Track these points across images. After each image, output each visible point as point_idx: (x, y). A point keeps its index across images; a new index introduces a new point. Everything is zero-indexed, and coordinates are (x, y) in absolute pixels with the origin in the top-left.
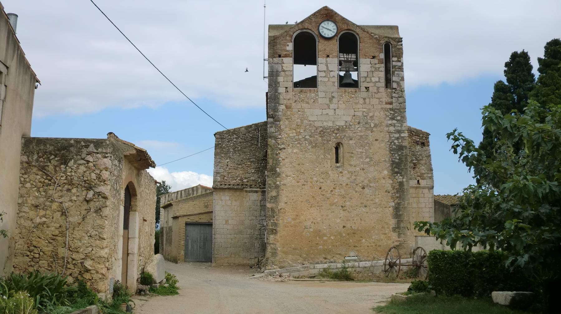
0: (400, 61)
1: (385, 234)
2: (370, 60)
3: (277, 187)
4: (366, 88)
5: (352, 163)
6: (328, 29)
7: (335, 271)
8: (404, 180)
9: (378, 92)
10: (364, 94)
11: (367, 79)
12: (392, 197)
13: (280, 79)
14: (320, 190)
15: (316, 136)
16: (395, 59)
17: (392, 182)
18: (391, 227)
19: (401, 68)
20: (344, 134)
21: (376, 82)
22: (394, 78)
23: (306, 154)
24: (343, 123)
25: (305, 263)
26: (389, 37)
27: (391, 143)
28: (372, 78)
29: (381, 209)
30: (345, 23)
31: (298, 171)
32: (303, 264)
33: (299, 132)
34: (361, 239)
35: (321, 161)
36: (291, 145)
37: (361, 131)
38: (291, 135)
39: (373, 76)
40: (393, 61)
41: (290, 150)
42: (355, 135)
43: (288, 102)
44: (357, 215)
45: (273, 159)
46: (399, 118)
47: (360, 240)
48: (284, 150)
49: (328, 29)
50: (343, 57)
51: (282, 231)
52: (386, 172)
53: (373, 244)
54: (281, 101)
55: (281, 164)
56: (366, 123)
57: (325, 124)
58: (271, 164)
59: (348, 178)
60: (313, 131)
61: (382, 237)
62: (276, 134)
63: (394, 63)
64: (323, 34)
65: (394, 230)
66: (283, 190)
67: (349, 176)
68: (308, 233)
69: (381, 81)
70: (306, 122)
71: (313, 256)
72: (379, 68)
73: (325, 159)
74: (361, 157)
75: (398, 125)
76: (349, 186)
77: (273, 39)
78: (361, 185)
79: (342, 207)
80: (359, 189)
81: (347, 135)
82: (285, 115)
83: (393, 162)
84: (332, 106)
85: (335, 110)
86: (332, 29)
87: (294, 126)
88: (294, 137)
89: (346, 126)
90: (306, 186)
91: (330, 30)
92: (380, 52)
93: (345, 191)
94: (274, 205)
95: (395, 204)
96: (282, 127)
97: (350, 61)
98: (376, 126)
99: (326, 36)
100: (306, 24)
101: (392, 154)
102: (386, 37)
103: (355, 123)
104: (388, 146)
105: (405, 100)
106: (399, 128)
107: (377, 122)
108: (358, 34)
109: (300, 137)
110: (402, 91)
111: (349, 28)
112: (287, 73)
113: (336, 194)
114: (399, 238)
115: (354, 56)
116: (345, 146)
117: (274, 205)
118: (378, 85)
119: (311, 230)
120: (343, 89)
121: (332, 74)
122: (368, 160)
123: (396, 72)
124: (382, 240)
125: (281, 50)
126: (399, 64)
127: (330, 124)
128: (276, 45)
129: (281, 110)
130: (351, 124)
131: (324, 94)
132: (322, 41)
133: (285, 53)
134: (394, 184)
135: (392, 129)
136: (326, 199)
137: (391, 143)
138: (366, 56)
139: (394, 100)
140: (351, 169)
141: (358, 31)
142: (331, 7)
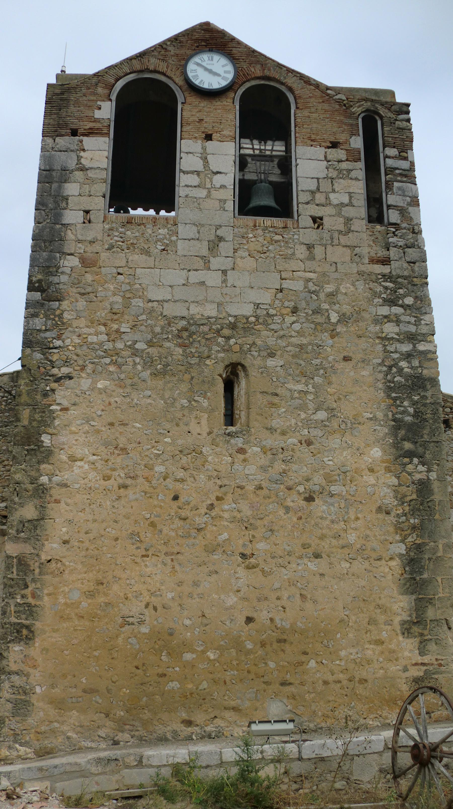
0: (406, 159)
1: (380, 642)
2: (323, 150)
3: (41, 492)
4: (314, 219)
5: (275, 423)
7: (213, 774)
8: (433, 476)
9: (349, 231)
10: (311, 235)
11: (318, 196)
12: (398, 528)
13: (71, 189)
14: (175, 504)
15: (167, 344)
17: (395, 481)
18: (397, 620)
19: (409, 175)
20: (250, 340)
21: (342, 205)
22: (391, 199)
23: (134, 395)
24: (247, 310)
25: (120, 736)
26: (372, 101)
27: (390, 367)
28: (332, 196)
29: (366, 564)
30: (258, 62)
31: (106, 444)
32: (116, 743)
33: (117, 331)
34: (303, 658)
35: (179, 415)
36: (90, 368)
37: (300, 333)
38: (92, 339)
39: (334, 191)
40: (386, 157)
41: (85, 383)
42: (282, 343)
43: (90, 249)
44: (292, 583)
45: (34, 406)
46: (409, 301)
47: (301, 664)
48: (67, 382)
50: (251, 147)
51: (50, 633)
52: (376, 453)
53: (341, 676)
54: (70, 247)
55: (57, 422)
56: (316, 312)
57: (194, 310)
58: (26, 422)
59: (264, 469)
60: (158, 329)
61: (371, 651)
62: (48, 334)
63: (390, 162)
64: (197, 82)
65: (407, 629)
66: (57, 501)
67: (264, 461)
68: (133, 641)
69: (355, 202)
70: (138, 302)
71: (146, 715)
73: (191, 409)
74: (303, 407)
75: (407, 318)
76: (265, 492)
77: (58, 91)
78: (301, 489)
79: (243, 556)
80: (295, 501)
81: (259, 342)
82: (76, 283)
83: (398, 424)
84: (215, 262)
85: (224, 272)
86: (222, 74)
87: (102, 314)
88: (101, 344)
89: (257, 317)
90: (130, 492)
91: (219, 75)
92: (352, 134)
93: (252, 507)
94: (27, 549)
95: (409, 550)
96: (66, 316)
97: (271, 158)
98: (344, 319)
99: (206, 86)
100: (153, 60)
101: (395, 399)
102: (366, 100)
103: (284, 311)
104: (381, 376)
105: (424, 253)
106: (413, 329)
107: (346, 309)
108: (291, 89)
109: (120, 345)
110: (416, 231)
111: (267, 73)
112: (90, 174)
113: (226, 515)
114: (422, 653)
115: (279, 147)
116: (253, 372)
117: (27, 549)
118: (348, 212)
119: (144, 629)
120: (249, 220)
121: (218, 180)
122: (322, 415)
123: (396, 184)
124: (369, 662)
125: (80, 119)
126: (404, 165)
127: (211, 311)
128: (67, 107)
129: (68, 270)
130: (272, 312)
131: (195, 229)
132: (193, 100)
134: (403, 489)
135: (390, 329)
136: (193, 532)
137: (390, 367)
138: (312, 141)
139: (393, 253)
140: (272, 441)
141: (290, 81)
142: (221, 23)
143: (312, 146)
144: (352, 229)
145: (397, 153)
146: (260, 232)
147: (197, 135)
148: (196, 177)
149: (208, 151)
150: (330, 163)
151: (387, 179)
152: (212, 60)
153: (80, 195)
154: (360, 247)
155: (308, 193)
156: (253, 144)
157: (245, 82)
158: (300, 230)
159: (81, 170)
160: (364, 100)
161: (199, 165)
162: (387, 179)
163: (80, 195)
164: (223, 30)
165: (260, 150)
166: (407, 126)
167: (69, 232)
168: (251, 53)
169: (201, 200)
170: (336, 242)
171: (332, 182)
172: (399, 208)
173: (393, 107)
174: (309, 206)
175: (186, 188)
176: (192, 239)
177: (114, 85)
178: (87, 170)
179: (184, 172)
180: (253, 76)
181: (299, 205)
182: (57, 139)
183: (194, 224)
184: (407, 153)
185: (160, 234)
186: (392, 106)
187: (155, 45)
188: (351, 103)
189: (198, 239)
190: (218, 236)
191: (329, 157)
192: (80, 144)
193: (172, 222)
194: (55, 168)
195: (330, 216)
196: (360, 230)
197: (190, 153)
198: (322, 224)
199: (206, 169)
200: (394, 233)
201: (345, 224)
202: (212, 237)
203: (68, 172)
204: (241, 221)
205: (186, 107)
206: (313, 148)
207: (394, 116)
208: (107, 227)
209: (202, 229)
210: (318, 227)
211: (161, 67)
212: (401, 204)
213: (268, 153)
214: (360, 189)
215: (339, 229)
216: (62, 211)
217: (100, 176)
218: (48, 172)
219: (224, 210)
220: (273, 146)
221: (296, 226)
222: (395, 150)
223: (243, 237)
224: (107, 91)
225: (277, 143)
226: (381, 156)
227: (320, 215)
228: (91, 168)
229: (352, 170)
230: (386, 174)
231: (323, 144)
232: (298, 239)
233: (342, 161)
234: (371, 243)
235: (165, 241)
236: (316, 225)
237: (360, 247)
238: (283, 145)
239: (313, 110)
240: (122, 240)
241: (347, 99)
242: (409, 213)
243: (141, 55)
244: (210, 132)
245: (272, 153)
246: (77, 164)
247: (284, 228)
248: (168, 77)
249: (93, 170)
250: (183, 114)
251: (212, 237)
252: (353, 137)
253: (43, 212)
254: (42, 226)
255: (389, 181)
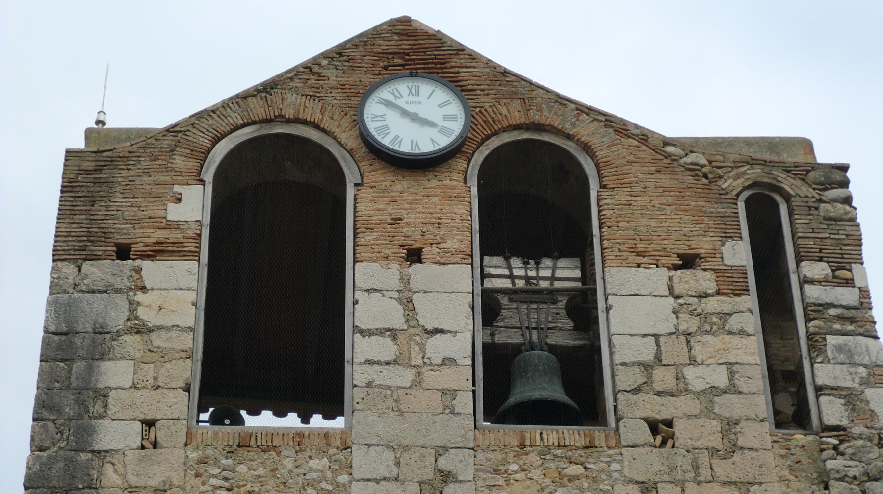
0: (849, 283)
2: (664, 273)
4: (654, 426)
6: (414, 118)
9: (734, 448)
10: (648, 462)
13: (115, 374)
16: (817, 270)
21: (715, 391)
22: (824, 373)
26: (765, 163)
28: (690, 373)
30: (514, 95)
39: (693, 361)
40: (805, 281)
49: (416, 117)
50: (505, 272)
63: (814, 293)
64: (386, 141)
69: (742, 384)
72: (725, 316)
77: (88, 165)
86: (440, 122)
97: (551, 295)
99: (405, 148)
100: (291, 98)
102: (752, 162)
108: (587, 148)
111: (535, 116)
112: (158, 340)
115: (568, 271)
120: (510, 433)
121: (437, 347)
123: (831, 340)
125: (135, 222)
126: (847, 296)
128: (107, 197)
131: (389, 456)
132: (380, 177)
133: (159, 235)
138: (640, 256)
141: (586, 131)
143: (639, 265)
144: (740, 443)
145: (828, 271)
146: (534, 458)
147: (388, 252)
148: (388, 341)
149: (414, 285)
150: (681, 301)
151: (811, 330)
152: (417, 94)
153: (134, 386)
154: (760, 483)
155: (636, 368)
156: (510, 268)
157: (488, 137)
158: (624, 450)
159: (137, 333)
160: (748, 163)
161: (396, 318)
162: (811, 330)
163: (134, 386)
164: (438, 31)
165: (527, 279)
166: (847, 213)
167: (109, 469)
168: (500, 77)
169: (401, 392)
170: (705, 474)
171: (688, 342)
172: (844, 393)
173: (812, 175)
174: (641, 396)
175: (367, 367)
176: (384, 479)
177: (209, 151)
178: (151, 331)
179: (362, 332)
180: (505, 124)
181: (619, 395)
182: (87, 266)
183: (388, 446)
184: (850, 270)
185: (311, 470)
186: (808, 171)
187: (296, 67)
188: (720, 171)
189: (396, 479)
190: (441, 471)
191: (678, 289)
192: (136, 276)
193: (338, 443)
194: (80, 328)
195: (689, 417)
196: (758, 446)
197: (376, 290)
198: (672, 436)
199: (412, 323)
200: (835, 448)
201: (724, 433)
202: (428, 474)
203: (108, 336)
204: (492, 435)
205: (364, 192)
206: (641, 269)
207: (814, 193)
208: (194, 455)
209: (406, 455)
210: (664, 443)
211: (309, 111)
212: (848, 384)
213: (544, 284)
214: (752, 354)
215: (710, 444)
216: (93, 422)
217: (178, 346)
218: (64, 338)
219: (453, 412)
220: (554, 269)
221: (613, 442)
222: (824, 265)
223: (497, 472)
224: (194, 164)
225: (562, 262)
226: (794, 279)
227: (665, 415)
228: (160, 328)
229: (730, 314)
230: (808, 320)
231: (664, 261)
232: (620, 472)
233: (707, 295)
234: (786, 473)
235: (324, 485)
236: (659, 438)
237: (760, 483)
238: (576, 267)
239: (637, 189)
240: (226, 484)
241: (710, 162)
242: (868, 402)
243: (267, 88)
244: (417, 245)
245: (552, 284)
246: (128, 319)
247: (587, 447)
248: (324, 131)
249: (163, 332)
250: (358, 209)
251: (428, 474)
252: (729, 244)
253: (50, 425)
254: (49, 457)
255: (816, 334)
